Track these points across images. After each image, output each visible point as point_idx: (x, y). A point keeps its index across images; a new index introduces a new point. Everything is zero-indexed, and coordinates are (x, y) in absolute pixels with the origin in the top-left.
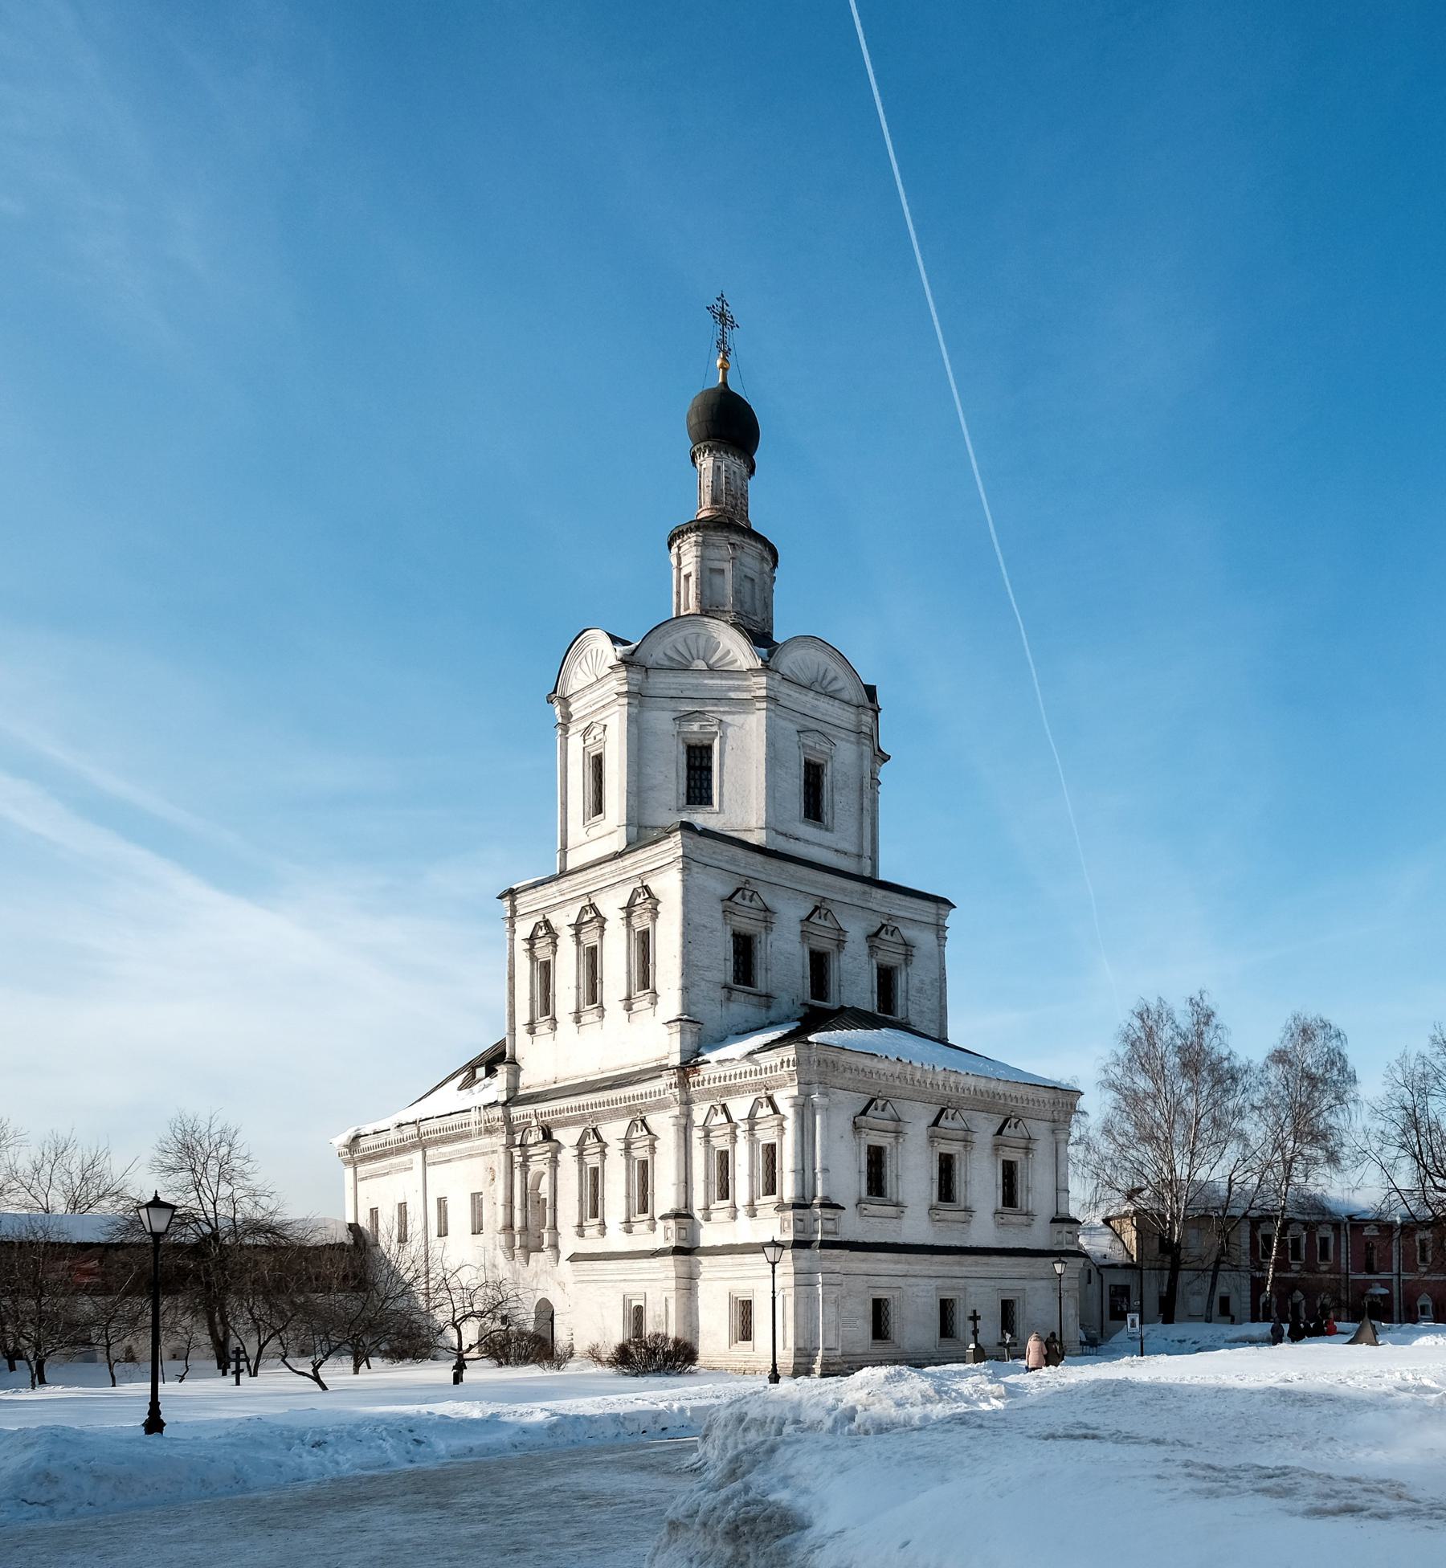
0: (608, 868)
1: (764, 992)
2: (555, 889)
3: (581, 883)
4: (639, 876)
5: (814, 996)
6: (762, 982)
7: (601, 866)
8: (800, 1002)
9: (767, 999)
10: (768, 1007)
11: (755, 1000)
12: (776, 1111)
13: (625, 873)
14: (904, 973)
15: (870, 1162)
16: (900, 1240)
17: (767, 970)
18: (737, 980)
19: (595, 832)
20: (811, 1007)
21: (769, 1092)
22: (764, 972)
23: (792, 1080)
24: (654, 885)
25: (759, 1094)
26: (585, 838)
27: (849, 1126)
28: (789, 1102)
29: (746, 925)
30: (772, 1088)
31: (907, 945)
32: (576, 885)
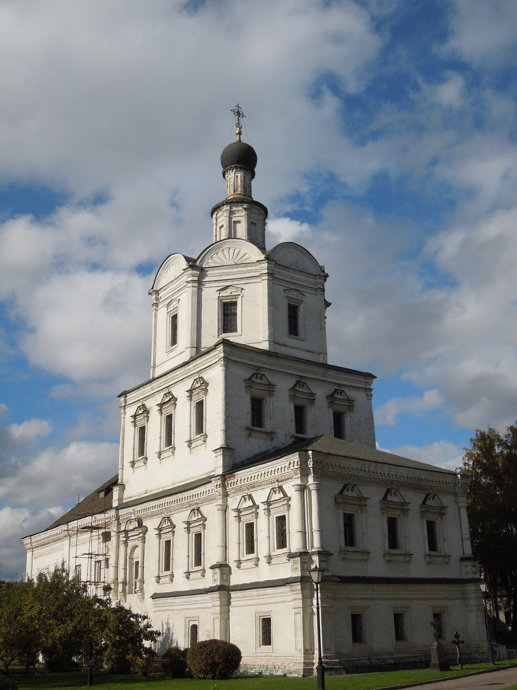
0: (179, 372)
1: (269, 431)
2: (149, 387)
3: (164, 382)
4: (198, 372)
5: (297, 432)
6: (268, 425)
7: (176, 371)
8: (290, 435)
9: (271, 435)
11: (264, 436)
12: (285, 495)
13: (189, 372)
15: (345, 525)
16: (367, 574)
18: (253, 425)
19: (172, 354)
20: (297, 438)
21: (280, 484)
23: (296, 474)
24: (206, 376)
25: (273, 486)
26: (166, 358)
27: (332, 501)
28: (293, 489)
29: (258, 393)
30: (283, 481)
32: (162, 383)
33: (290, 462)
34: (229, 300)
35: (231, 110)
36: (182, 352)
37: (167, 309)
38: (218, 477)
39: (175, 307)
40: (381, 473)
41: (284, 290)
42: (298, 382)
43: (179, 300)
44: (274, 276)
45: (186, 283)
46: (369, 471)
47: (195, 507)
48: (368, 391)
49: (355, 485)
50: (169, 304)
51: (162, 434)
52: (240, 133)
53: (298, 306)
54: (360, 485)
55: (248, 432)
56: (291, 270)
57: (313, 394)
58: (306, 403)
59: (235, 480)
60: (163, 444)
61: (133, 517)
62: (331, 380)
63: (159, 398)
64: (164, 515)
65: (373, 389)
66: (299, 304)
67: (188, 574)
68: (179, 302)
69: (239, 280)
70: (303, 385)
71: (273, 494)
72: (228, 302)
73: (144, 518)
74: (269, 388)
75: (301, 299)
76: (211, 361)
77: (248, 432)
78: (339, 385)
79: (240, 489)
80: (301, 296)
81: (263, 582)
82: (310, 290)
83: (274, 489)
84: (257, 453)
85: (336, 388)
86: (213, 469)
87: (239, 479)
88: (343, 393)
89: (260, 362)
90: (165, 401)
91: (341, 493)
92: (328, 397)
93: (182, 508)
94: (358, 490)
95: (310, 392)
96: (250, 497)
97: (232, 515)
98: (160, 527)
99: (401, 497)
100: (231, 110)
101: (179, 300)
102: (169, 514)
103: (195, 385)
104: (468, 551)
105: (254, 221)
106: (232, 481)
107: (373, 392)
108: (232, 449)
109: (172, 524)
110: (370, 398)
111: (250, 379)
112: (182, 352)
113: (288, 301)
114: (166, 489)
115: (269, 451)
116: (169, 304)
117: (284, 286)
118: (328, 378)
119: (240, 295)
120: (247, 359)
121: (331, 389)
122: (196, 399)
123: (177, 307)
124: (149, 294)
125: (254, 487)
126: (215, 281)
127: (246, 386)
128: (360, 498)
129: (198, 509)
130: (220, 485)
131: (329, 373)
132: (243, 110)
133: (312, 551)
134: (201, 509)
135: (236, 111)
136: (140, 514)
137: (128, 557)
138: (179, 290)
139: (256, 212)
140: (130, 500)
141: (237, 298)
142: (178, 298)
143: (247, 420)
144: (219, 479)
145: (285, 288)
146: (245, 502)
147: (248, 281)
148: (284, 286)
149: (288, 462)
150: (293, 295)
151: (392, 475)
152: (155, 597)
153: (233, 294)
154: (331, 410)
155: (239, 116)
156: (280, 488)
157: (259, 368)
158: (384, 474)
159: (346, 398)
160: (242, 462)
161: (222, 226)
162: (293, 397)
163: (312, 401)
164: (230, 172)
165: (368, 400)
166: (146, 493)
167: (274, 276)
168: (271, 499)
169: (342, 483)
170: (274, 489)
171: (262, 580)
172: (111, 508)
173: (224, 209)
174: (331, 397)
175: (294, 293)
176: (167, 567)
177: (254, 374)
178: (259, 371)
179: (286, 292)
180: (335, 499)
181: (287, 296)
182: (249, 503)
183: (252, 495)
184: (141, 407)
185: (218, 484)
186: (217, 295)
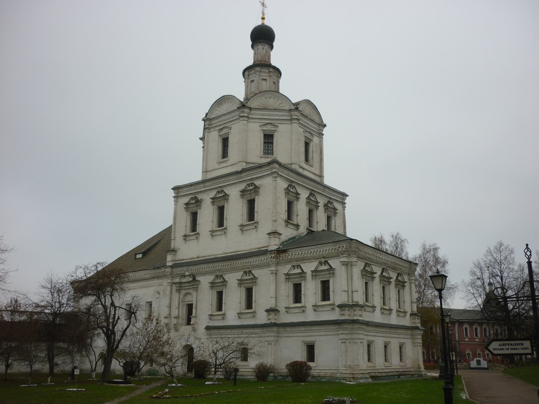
1: (296, 224)
4: (250, 179)
10: (298, 229)
11: (293, 227)
14: (334, 219)
17: (297, 215)
21: (326, 260)
22: (296, 216)
25: (320, 260)
26: (217, 166)
30: (329, 258)
31: (335, 209)
32: (214, 183)
33: (339, 246)
34: (268, 133)
35: (260, 2)
36: (234, 164)
37: (219, 133)
38: (273, 252)
39: (226, 132)
40: (381, 258)
41: (304, 131)
42: (311, 194)
43: (231, 128)
44: (300, 121)
45: (239, 117)
46: (377, 256)
47: (247, 270)
48: (343, 204)
49: (370, 264)
50: (220, 130)
51: (214, 218)
52: (263, 18)
53: (309, 143)
54: (372, 265)
55: (286, 224)
56: (307, 119)
57: (318, 202)
58: (314, 208)
59: (287, 255)
60: (214, 226)
61: (187, 273)
62: (326, 194)
63: (213, 194)
64: (216, 274)
65: (346, 203)
66: (310, 142)
67: (240, 315)
68: (230, 129)
69: (276, 121)
70: (313, 196)
71: (319, 266)
72: (267, 134)
73: (197, 275)
74: (296, 196)
75: (311, 139)
76: (262, 173)
77: (286, 224)
78: (330, 198)
79: (290, 261)
80: (312, 137)
81: (309, 322)
82: (316, 134)
83: (321, 263)
84: (290, 238)
85: (329, 200)
86: (267, 245)
87: (291, 254)
88: (332, 204)
89: (292, 178)
90: (217, 196)
91: (364, 268)
92: (324, 205)
93: (234, 270)
94: (371, 267)
95: (316, 201)
96: (299, 266)
97: (282, 278)
98: (213, 282)
99: (388, 274)
100: (260, 2)
101: (231, 128)
102: (221, 273)
103: (247, 188)
104: (415, 309)
105: (275, 81)
106: (284, 255)
107: (346, 205)
108: (280, 233)
109: (224, 280)
110: (344, 209)
111: (287, 188)
112: (234, 164)
113: (305, 139)
114: (218, 256)
115: (295, 237)
116: (220, 130)
117: (304, 129)
118: (324, 193)
119: (276, 130)
120: (286, 175)
121: (326, 200)
122: (249, 197)
123: (229, 132)
124: (203, 120)
125: (303, 260)
126: (259, 118)
127: (285, 193)
128: (372, 272)
129: (250, 271)
130: (274, 257)
131: (326, 190)
132: (266, 3)
133: (354, 303)
134: (253, 272)
135: (262, 2)
136: (194, 272)
137: (180, 301)
138: (231, 121)
139: (276, 75)
140: (182, 261)
141: (274, 133)
142: (230, 126)
143: (284, 216)
144: (274, 253)
145: (304, 131)
146: (294, 269)
147: (282, 122)
148: (304, 129)
149: (338, 246)
150: (308, 135)
151: (386, 260)
152: (208, 328)
153: (271, 129)
154: (326, 214)
155: (264, 7)
156: (326, 262)
157: (292, 181)
158: (383, 259)
159: (333, 207)
160: (283, 243)
161: (253, 81)
162: (308, 203)
163: (317, 207)
164: (259, 44)
165: (343, 210)
166: (198, 258)
167: (300, 121)
168: (318, 269)
169: (364, 262)
170: (321, 263)
171: (308, 321)
172: (165, 266)
173: (256, 69)
174: (326, 206)
175: (308, 134)
176: (220, 308)
177: (289, 185)
178: (292, 184)
179: (304, 133)
180: (361, 272)
181: (305, 136)
182: (298, 271)
183: (301, 265)
184: (193, 198)
185: (273, 256)
186: (260, 129)
